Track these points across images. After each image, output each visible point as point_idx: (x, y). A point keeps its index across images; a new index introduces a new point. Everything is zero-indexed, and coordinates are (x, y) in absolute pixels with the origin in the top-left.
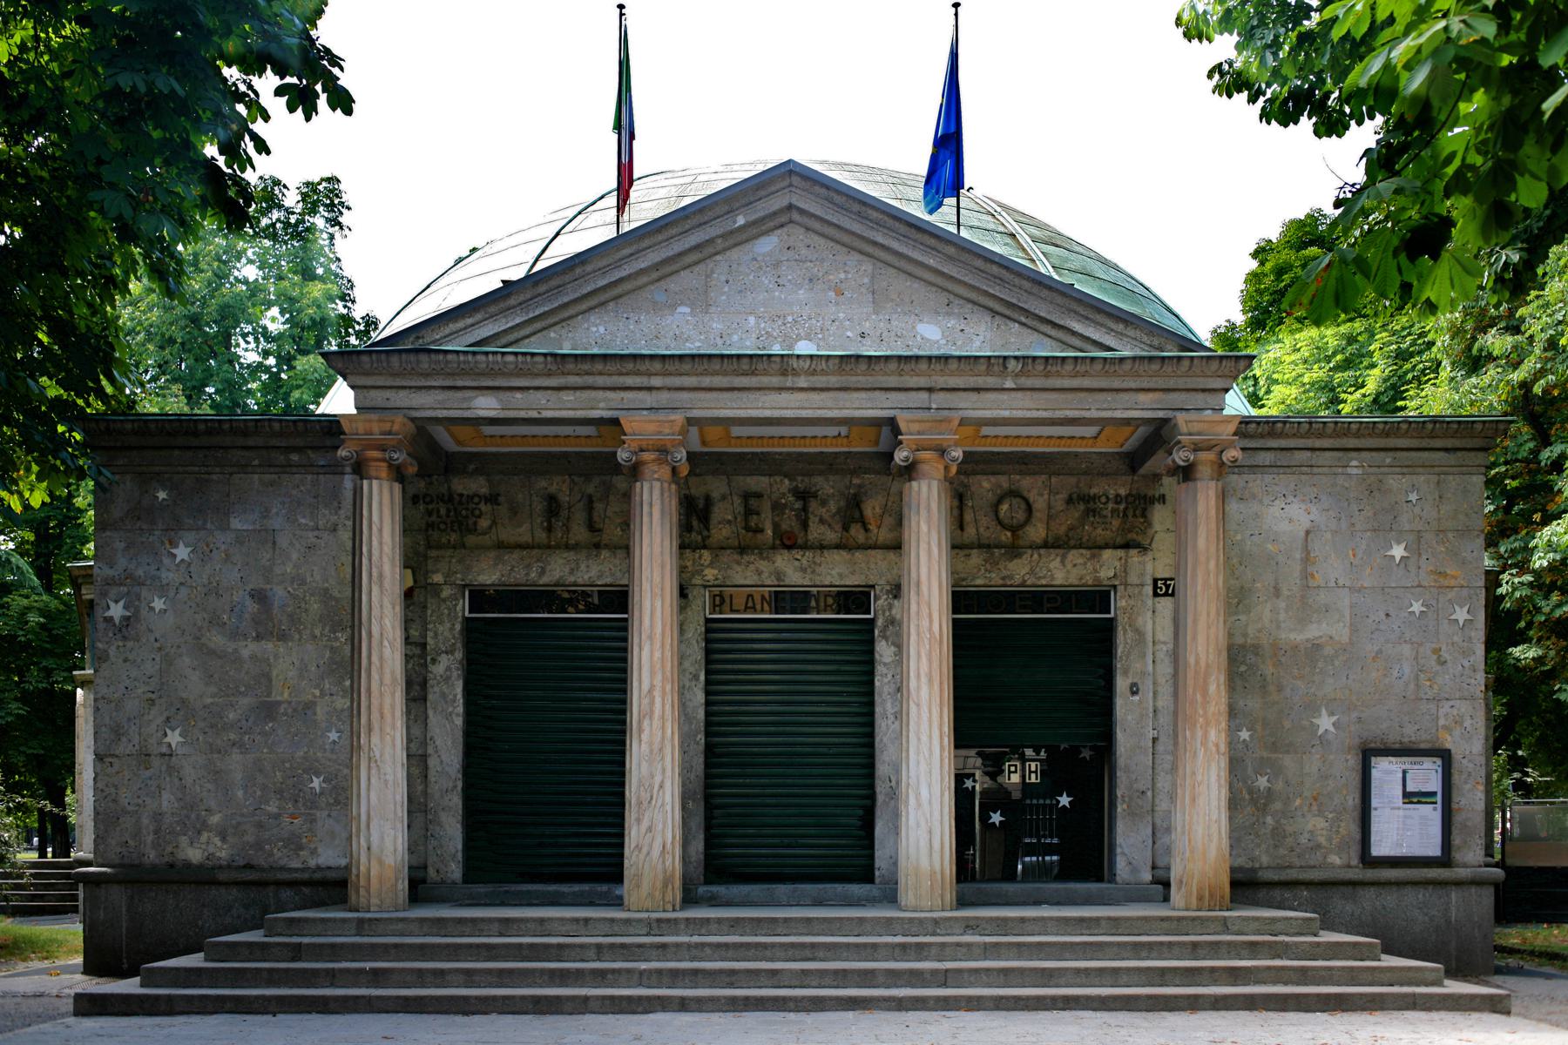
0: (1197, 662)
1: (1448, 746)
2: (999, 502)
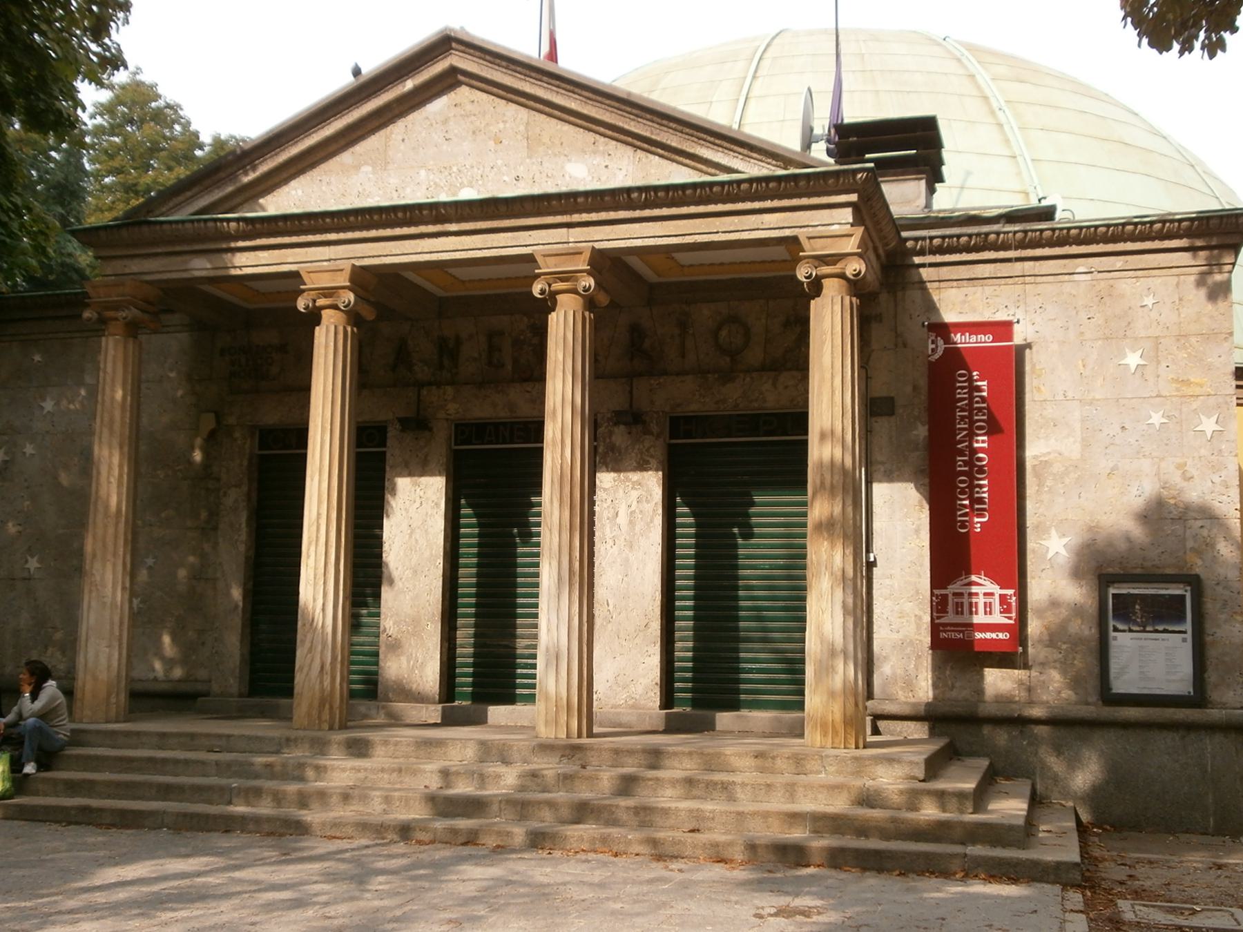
1: (1197, 571)
2: (719, 328)
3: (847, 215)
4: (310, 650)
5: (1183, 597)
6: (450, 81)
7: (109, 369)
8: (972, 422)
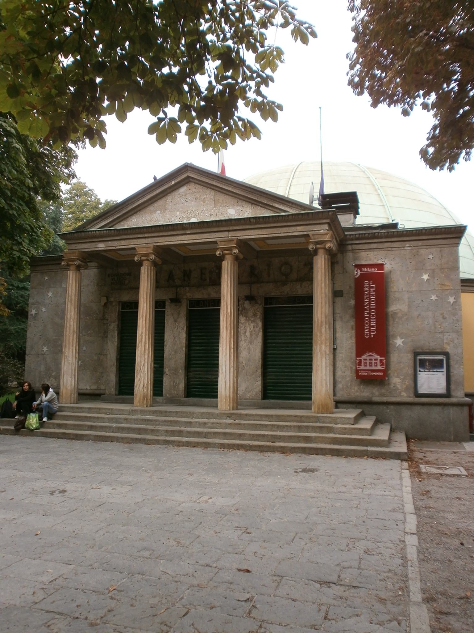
0: (318, 321)
1: (448, 350)
3: (326, 227)
4: (140, 379)
5: (442, 360)
6: (187, 181)
7: (71, 282)
8: (370, 299)
